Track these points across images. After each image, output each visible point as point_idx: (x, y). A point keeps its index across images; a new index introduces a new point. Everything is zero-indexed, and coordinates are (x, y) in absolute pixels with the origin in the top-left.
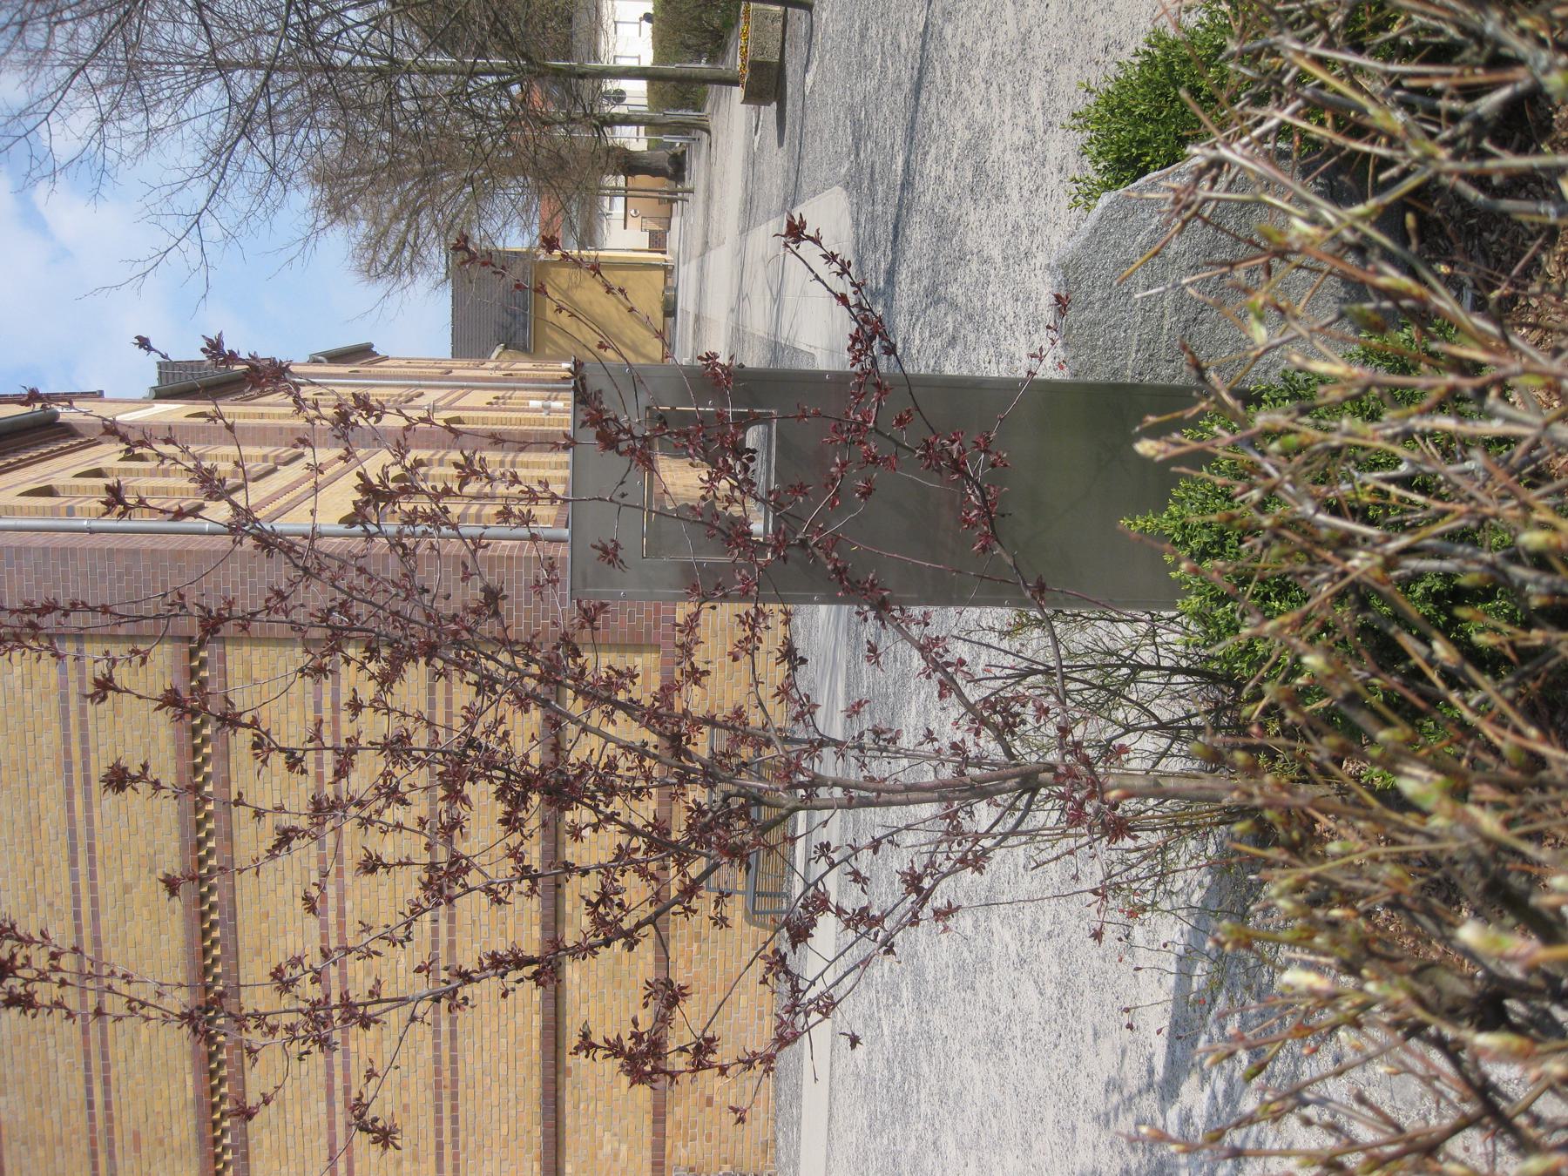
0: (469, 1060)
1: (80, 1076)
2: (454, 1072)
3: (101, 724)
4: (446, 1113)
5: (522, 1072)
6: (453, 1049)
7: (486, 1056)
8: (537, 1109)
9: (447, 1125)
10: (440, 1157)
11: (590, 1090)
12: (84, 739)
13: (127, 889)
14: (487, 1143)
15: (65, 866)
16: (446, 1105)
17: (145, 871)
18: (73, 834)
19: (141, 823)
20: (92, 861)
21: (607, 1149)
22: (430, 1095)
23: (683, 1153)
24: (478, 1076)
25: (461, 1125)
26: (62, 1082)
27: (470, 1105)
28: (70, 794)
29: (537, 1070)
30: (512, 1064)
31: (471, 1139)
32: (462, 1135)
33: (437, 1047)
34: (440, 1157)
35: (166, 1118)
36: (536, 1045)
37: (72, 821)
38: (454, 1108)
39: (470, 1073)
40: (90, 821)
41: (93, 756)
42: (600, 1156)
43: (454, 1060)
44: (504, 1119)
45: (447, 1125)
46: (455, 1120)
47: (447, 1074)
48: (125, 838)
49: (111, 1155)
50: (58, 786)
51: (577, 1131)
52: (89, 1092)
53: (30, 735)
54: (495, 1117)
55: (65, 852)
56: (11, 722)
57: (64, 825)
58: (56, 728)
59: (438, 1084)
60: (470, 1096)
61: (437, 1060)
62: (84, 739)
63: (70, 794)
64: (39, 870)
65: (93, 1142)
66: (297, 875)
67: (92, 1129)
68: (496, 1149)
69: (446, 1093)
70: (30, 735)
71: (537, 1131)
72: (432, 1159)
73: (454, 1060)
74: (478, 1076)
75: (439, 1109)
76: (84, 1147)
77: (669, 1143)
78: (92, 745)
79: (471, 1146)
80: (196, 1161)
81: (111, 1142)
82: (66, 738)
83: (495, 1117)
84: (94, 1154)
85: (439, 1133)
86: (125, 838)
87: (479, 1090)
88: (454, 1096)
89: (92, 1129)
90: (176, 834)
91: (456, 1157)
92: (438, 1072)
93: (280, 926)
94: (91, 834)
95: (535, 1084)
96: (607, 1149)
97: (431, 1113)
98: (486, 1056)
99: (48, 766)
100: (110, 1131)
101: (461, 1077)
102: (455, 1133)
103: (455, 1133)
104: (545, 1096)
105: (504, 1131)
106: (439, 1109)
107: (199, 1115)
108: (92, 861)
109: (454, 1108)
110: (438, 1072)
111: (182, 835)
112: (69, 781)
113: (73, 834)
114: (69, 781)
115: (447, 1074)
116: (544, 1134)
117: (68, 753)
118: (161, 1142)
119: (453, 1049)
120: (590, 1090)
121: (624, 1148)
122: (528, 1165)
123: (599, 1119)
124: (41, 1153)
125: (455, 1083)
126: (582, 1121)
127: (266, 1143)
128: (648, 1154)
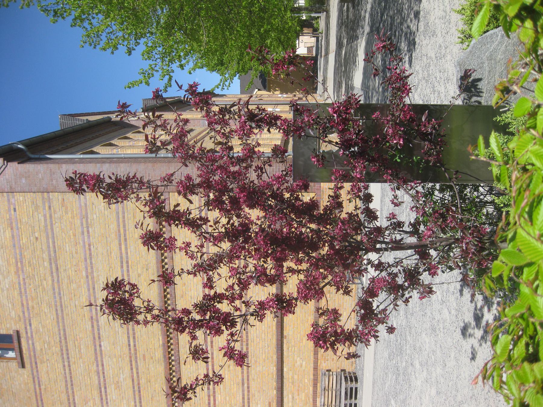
0: (252, 333)
1: (126, 336)
3: (130, 221)
5: (270, 337)
7: (258, 332)
8: (275, 350)
12: (124, 226)
13: (139, 275)
14: (258, 361)
15: (119, 268)
17: (145, 270)
18: (122, 258)
19: (143, 254)
20: (128, 267)
21: (298, 363)
23: (324, 365)
24: (255, 338)
26: (120, 338)
27: (252, 348)
28: (120, 244)
30: (266, 334)
31: (253, 359)
35: (153, 350)
36: (274, 328)
37: (121, 253)
39: (252, 337)
40: (127, 253)
41: (127, 232)
42: (296, 366)
44: (264, 353)
48: (138, 259)
49: (136, 362)
50: (117, 242)
51: (288, 357)
52: (129, 341)
53: (107, 225)
54: (261, 352)
55: (119, 264)
56: (101, 221)
57: (119, 255)
58: (115, 223)
60: (252, 344)
62: (124, 226)
63: (120, 244)
64: (111, 270)
65: (130, 357)
67: (130, 353)
68: (261, 362)
70: (107, 225)
71: (275, 357)
74: (255, 338)
76: (128, 359)
77: (319, 361)
78: (127, 228)
79: (253, 361)
80: (163, 364)
81: (136, 358)
82: (119, 226)
83: (261, 352)
84: (131, 361)
86: (138, 259)
87: (255, 343)
89: (130, 353)
90: (155, 258)
93: (189, 288)
94: (127, 258)
95: (274, 341)
96: (298, 363)
98: (258, 332)
99: (113, 236)
100: (136, 354)
101: (249, 338)
105: (264, 357)
107: (164, 349)
108: (128, 267)
111: (157, 258)
112: (120, 240)
113: (122, 258)
114: (120, 240)
116: (277, 358)
117: (119, 231)
118: (152, 358)
120: (293, 344)
121: (304, 363)
122: (272, 368)
123: (296, 353)
124: (115, 360)
125: (247, 340)
126: (290, 354)
128: (312, 365)
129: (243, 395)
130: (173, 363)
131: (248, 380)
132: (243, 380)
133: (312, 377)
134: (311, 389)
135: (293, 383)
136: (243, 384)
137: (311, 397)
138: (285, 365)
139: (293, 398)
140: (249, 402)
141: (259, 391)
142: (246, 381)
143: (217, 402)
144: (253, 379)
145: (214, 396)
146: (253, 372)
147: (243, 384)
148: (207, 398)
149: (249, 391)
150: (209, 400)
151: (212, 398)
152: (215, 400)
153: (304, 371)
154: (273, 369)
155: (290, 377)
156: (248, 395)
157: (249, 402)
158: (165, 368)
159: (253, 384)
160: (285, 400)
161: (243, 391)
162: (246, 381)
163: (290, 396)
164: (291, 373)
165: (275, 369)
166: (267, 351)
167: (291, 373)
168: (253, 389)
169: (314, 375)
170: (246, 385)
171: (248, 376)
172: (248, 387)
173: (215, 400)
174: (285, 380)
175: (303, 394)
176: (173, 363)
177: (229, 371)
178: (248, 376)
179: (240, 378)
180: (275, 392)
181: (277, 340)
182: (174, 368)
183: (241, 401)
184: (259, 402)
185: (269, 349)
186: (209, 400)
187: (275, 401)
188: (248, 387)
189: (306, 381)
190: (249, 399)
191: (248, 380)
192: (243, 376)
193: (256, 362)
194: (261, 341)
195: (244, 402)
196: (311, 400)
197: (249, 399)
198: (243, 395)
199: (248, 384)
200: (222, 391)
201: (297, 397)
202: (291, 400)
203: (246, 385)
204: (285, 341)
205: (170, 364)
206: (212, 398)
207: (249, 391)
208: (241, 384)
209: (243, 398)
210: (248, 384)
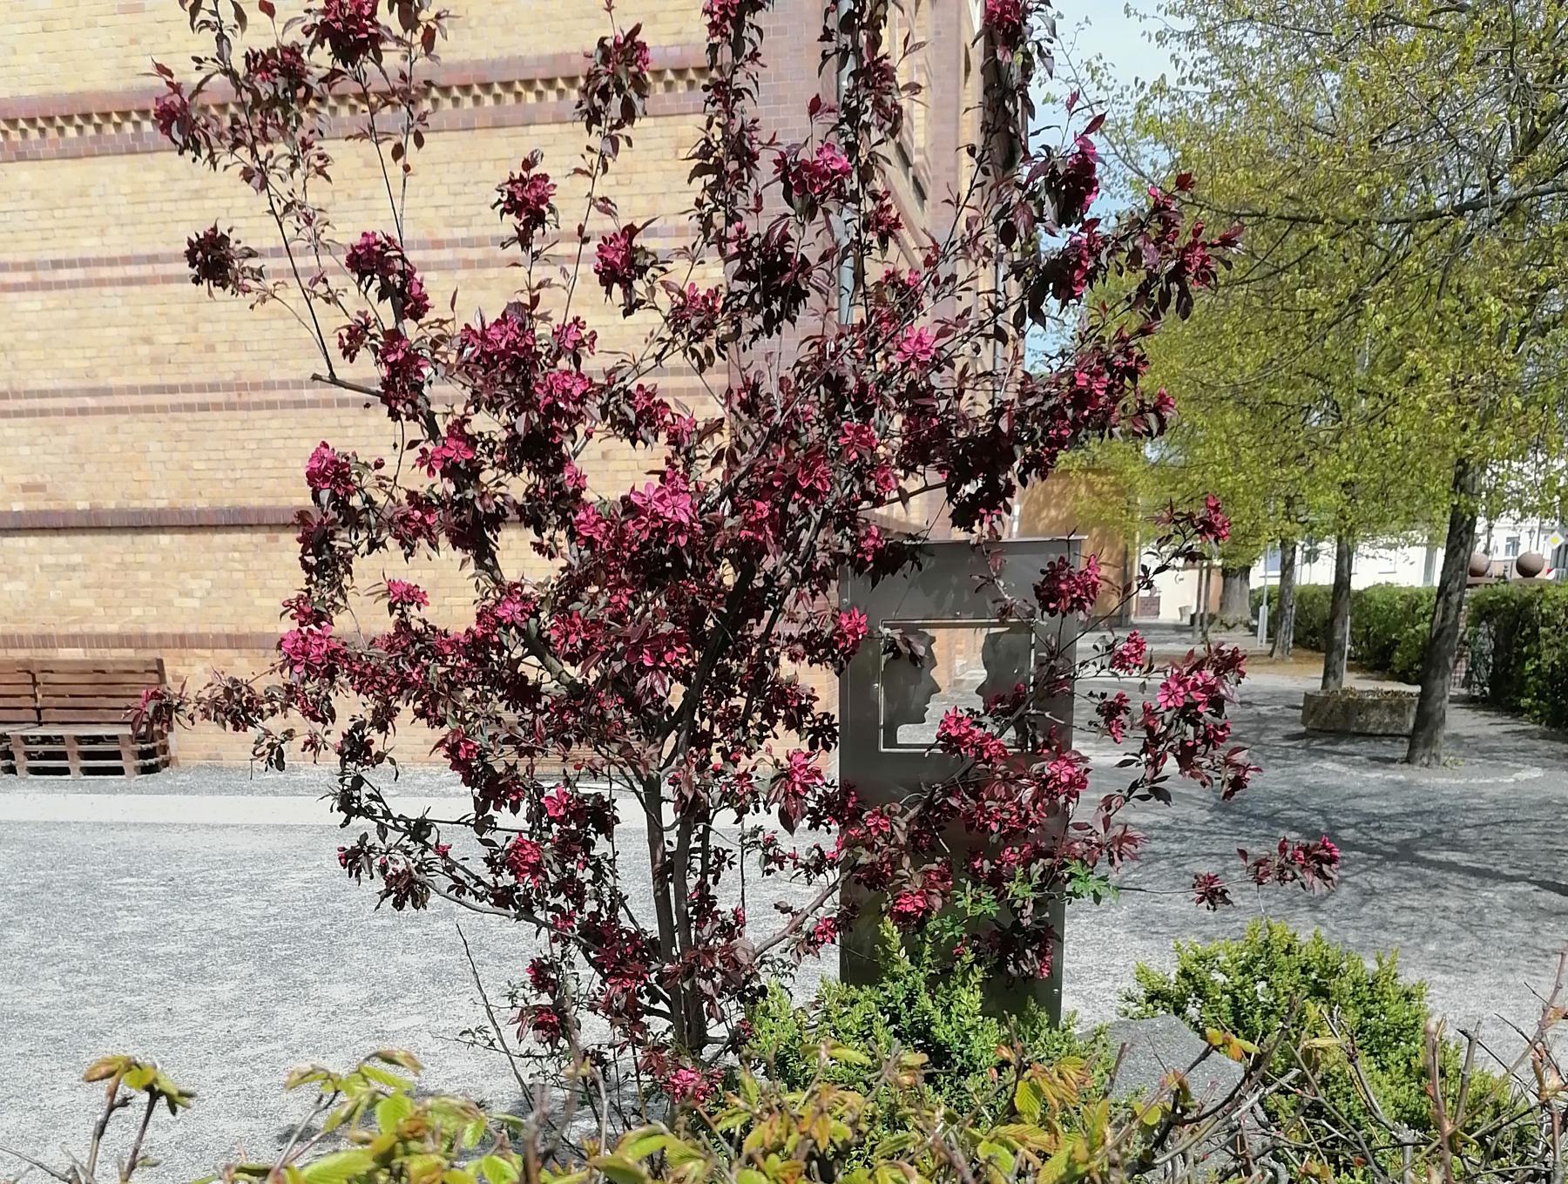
2: (258, 406)
4: (210, 397)
5: (269, 485)
6: (284, 405)
8: (227, 504)
9: (194, 398)
10: (160, 389)
11: (255, 564)
14: (183, 446)
16: (220, 397)
21: (193, 584)
22: (229, 377)
23: (199, 669)
24: (257, 434)
25: (199, 415)
27: (222, 424)
29: (270, 502)
30: (274, 473)
31: (183, 427)
32: (187, 416)
33: (284, 385)
34: (160, 389)
38: (217, 407)
39: (258, 424)
42: (183, 576)
43: (271, 405)
44: (211, 465)
45: (194, 398)
46: (204, 407)
47: (256, 397)
51: (208, 549)
54: (213, 455)
59: (242, 387)
61: (269, 386)
66: (461, 210)
68: (176, 456)
69: (234, 396)
71: (202, 504)
72: (155, 381)
73: (271, 405)
74: (257, 434)
75: (214, 388)
77: (208, 653)
79: (177, 427)
80: (119, 86)
83: (213, 455)
85: (187, 388)
87: (241, 435)
88: (231, 406)
91: (163, 409)
92: (255, 387)
95: (255, 501)
96: (193, 584)
97: (207, 379)
98: (280, 443)
101: (254, 414)
102: (189, 408)
103: (189, 408)
104: (243, 511)
105: (197, 465)
106: (214, 388)
109: (217, 407)
110: (255, 387)
111: (494, 63)
115: (256, 397)
116: (200, 512)
119: (284, 405)
120: (255, 564)
121: (196, 603)
122: (164, 494)
123: (224, 574)
125: (246, 407)
126: (220, 556)
127: (149, 176)
128: (191, 629)
129: (55, 394)
130: (129, 128)
131: (110, 410)
132: (108, 391)
133: (153, 629)
134: (113, 628)
135: (123, 566)
136: (93, 392)
137: (86, 628)
138: (180, 538)
139: (73, 568)
140: (31, 413)
141: (75, 449)
142: (105, 401)
143: (12, 296)
144: (115, 429)
145: (32, 287)
146: (141, 428)
147: (93, 392)
148: (22, 258)
149: (69, 412)
150: (17, 267)
151: (24, 277)
152: (18, 288)
153: (170, 603)
154: (159, 498)
155: (140, 558)
156: (57, 412)
157: (31, 413)
158: (108, 95)
159: (100, 425)
160: (60, 541)
161: (69, 393)
162: (105, 401)
163: (77, 559)
164: (155, 559)
165: (162, 504)
166: (220, 475)
167: (155, 559)
168: (74, 425)
169: (160, 636)
170: (90, 402)
171: (122, 410)
172: (83, 411)
173: (18, 288)
174: (126, 539)
175: (89, 603)
176: (129, 128)
177: (132, 341)
178: (122, 410)
179: (114, 382)
180: (82, 505)
181: (261, 511)
182: (110, 129)
183: (32, 385)
184: (38, 450)
185: (226, 484)
186: (17, 267)
187: (52, 506)
188: (83, 411)
189: (136, 612)
190: (44, 413)
191: (110, 410)
192: (120, 391)
193: (178, 437)
194: (248, 455)
195: (29, 394)
196: (74, 629)
197: (44, 413)
198: (55, 394)
199: (97, 411)
200: (58, 315)
201: (76, 583)
202: (63, 560)
203: (90, 402)
204: (259, 537)
205: (125, 115)
206: (24, 277)
207: (69, 412)
208: (90, 384)
209: (43, 394)
210: (97, 411)
